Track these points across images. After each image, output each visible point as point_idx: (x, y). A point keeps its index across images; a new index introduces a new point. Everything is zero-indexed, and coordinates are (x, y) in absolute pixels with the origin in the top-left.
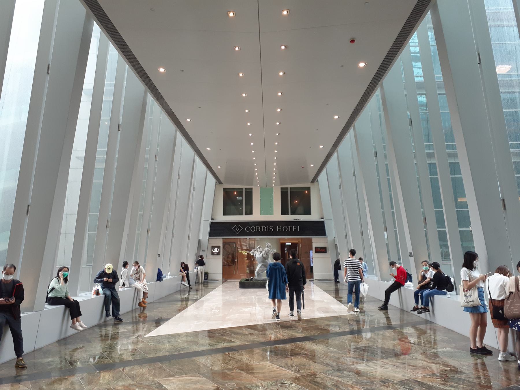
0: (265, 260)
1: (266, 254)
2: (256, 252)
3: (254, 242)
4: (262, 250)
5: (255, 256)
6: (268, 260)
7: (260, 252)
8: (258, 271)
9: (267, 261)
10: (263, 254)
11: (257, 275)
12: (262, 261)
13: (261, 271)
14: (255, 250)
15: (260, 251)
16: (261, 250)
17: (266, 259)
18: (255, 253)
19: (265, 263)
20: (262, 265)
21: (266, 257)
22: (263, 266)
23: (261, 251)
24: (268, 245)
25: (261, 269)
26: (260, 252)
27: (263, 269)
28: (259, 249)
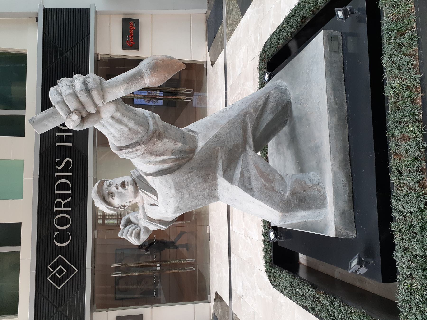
0: (196, 157)
1: (159, 145)
2: (140, 215)
3: (114, 217)
4: (127, 179)
5: (161, 222)
6: (194, 140)
7: (136, 192)
8: (274, 205)
9: (201, 144)
10: (153, 168)
11: (305, 209)
12: (205, 179)
13: (277, 187)
14: (129, 222)
15: (130, 188)
16: (123, 185)
17: (193, 151)
18: (143, 223)
19: (216, 159)
20: (230, 180)
21: (179, 145)
22: (238, 172)
23: (135, 183)
24: (73, 105)
25: (255, 184)
26: (141, 193)
27: (253, 172)
28: (116, 201)
